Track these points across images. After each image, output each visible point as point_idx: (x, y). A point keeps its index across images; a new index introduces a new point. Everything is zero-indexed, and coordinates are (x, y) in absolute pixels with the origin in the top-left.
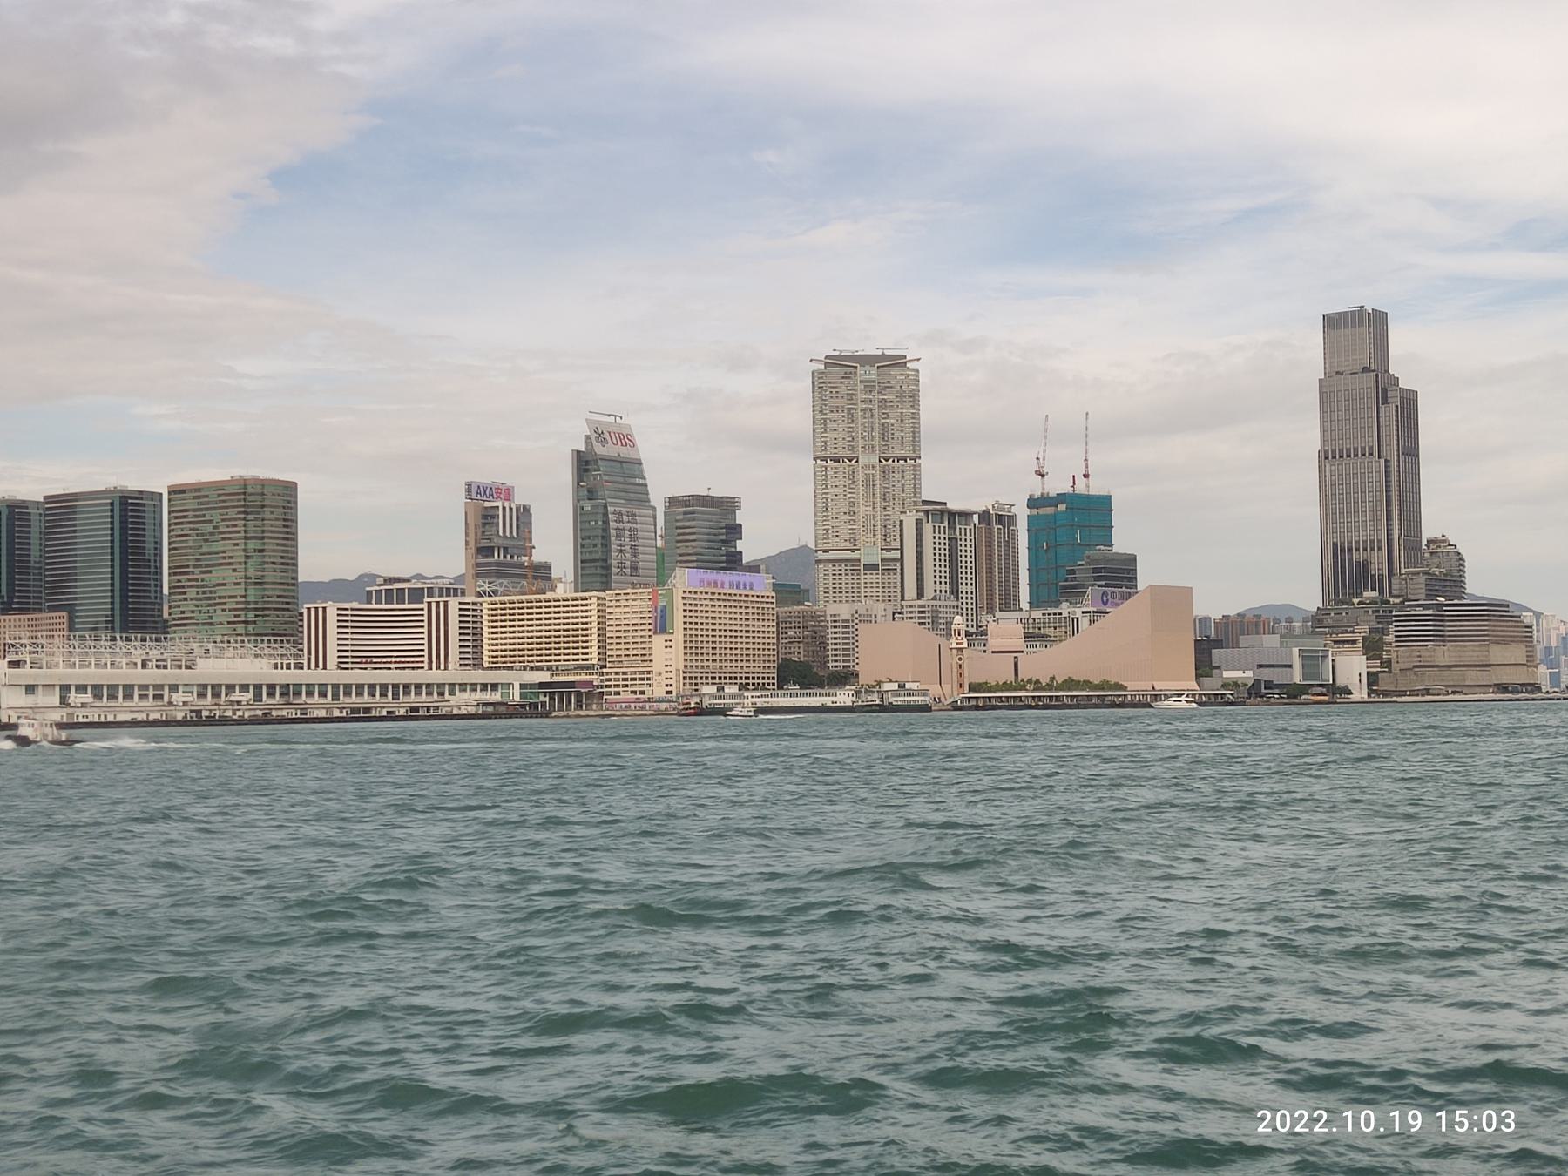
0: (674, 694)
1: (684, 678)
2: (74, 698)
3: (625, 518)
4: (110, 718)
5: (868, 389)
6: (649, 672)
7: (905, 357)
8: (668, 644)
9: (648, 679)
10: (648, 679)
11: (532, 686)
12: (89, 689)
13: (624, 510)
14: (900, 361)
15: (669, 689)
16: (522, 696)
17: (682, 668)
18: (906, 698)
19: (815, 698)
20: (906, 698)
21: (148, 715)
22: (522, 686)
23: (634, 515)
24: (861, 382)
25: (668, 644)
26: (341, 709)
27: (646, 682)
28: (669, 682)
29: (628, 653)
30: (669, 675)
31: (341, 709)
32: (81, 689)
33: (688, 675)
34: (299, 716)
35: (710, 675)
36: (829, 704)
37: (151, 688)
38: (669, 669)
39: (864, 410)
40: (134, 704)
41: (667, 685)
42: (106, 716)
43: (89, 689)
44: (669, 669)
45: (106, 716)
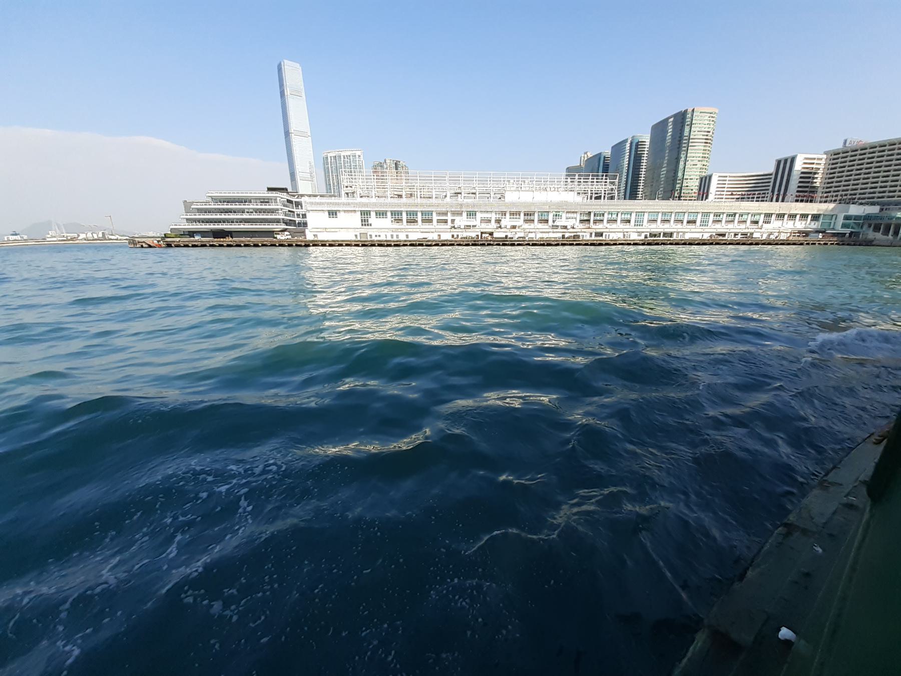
2: (373, 219)
4: (402, 237)
11: (857, 218)
12: (389, 214)
16: (844, 226)
21: (439, 236)
22: (847, 218)
26: (640, 233)
31: (640, 233)
32: (381, 214)
34: (593, 238)
37: (449, 214)
40: (418, 227)
42: (397, 236)
43: (389, 214)
45: (397, 236)
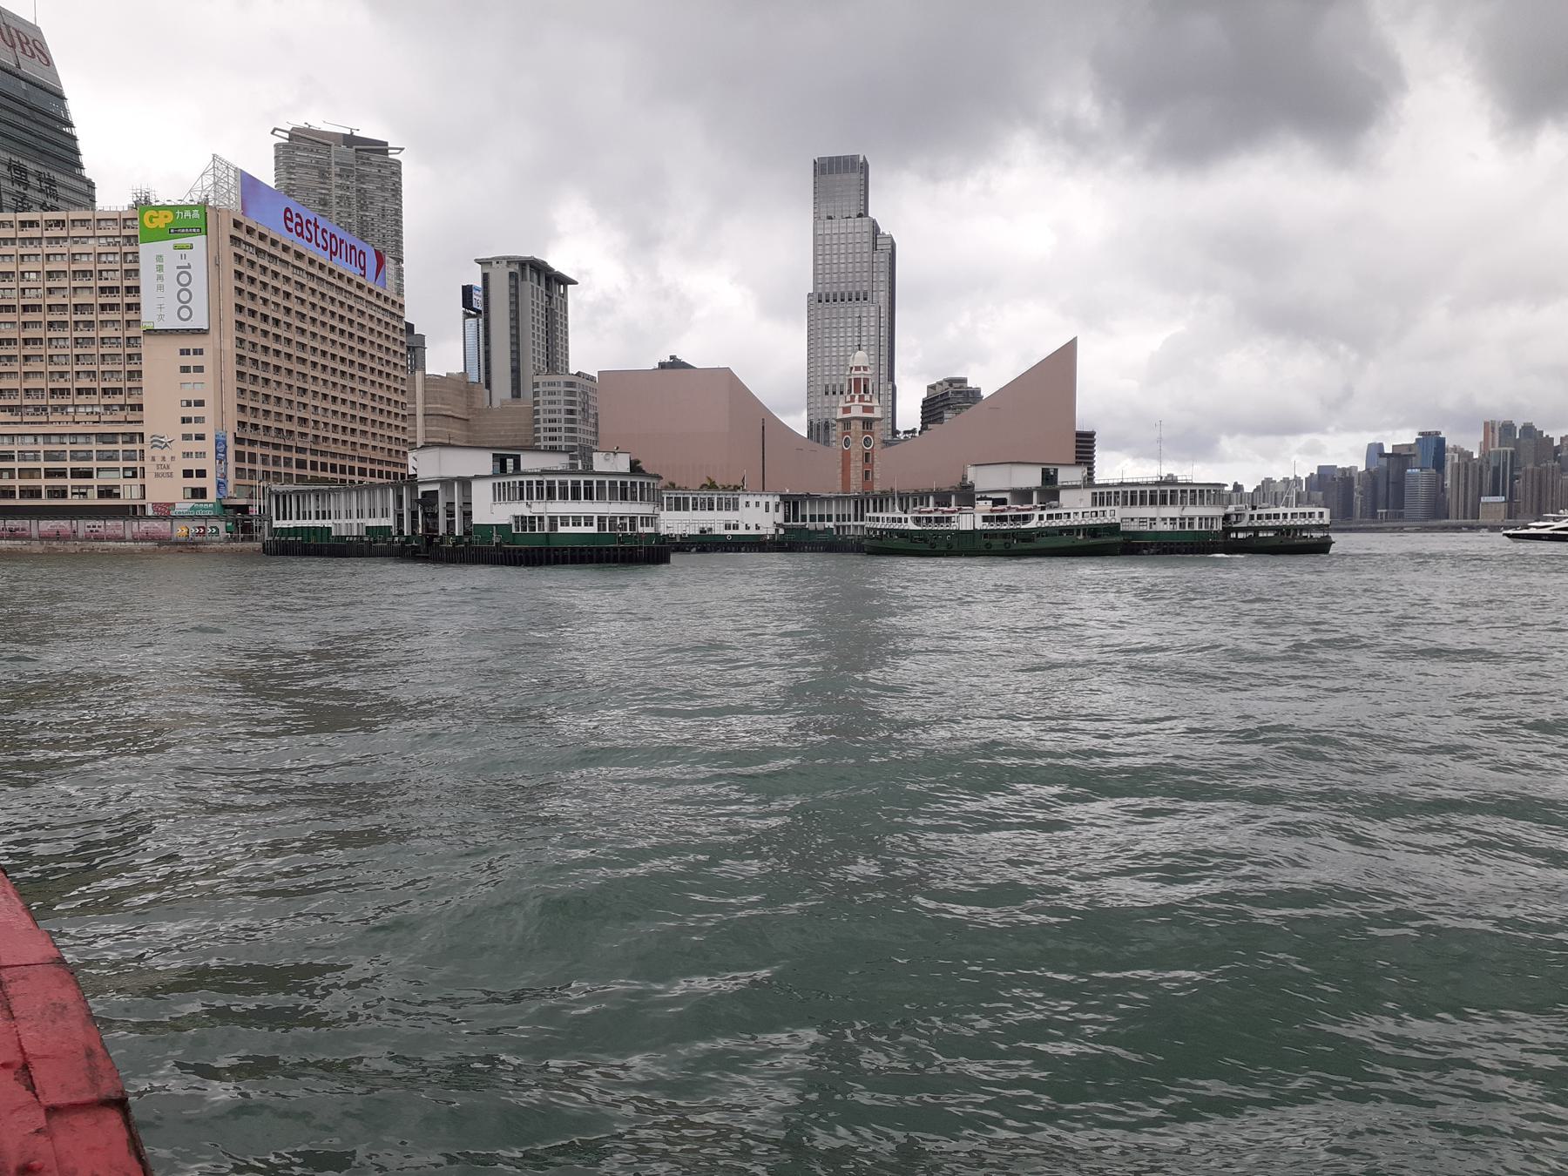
0: (212, 496)
1: (239, 456)
3: (32, 180)
5: (345, 174)
6: (131, 437)
7: (386, 144)
8: (191, 361)
9: (129, 456)
10: (129, 456)
13: (31, 167)
14: (380, 148)
15: (196, 482)
17: (231, 429)
18: (1191, 511)
19: (682, 514)
20: (1191, 511)
23: (51, 182)
24: (337, 163)
25: (191, 361)
27: (121, 464)
28: (194, 465)
29: (61, 384)
30: (194, 446)
33: (247, 449)
35: (295, 456)
36: (719, 530)
38: (193, 429)
39: (340, 197)
41: (187, 474)
44: (193, 429)
